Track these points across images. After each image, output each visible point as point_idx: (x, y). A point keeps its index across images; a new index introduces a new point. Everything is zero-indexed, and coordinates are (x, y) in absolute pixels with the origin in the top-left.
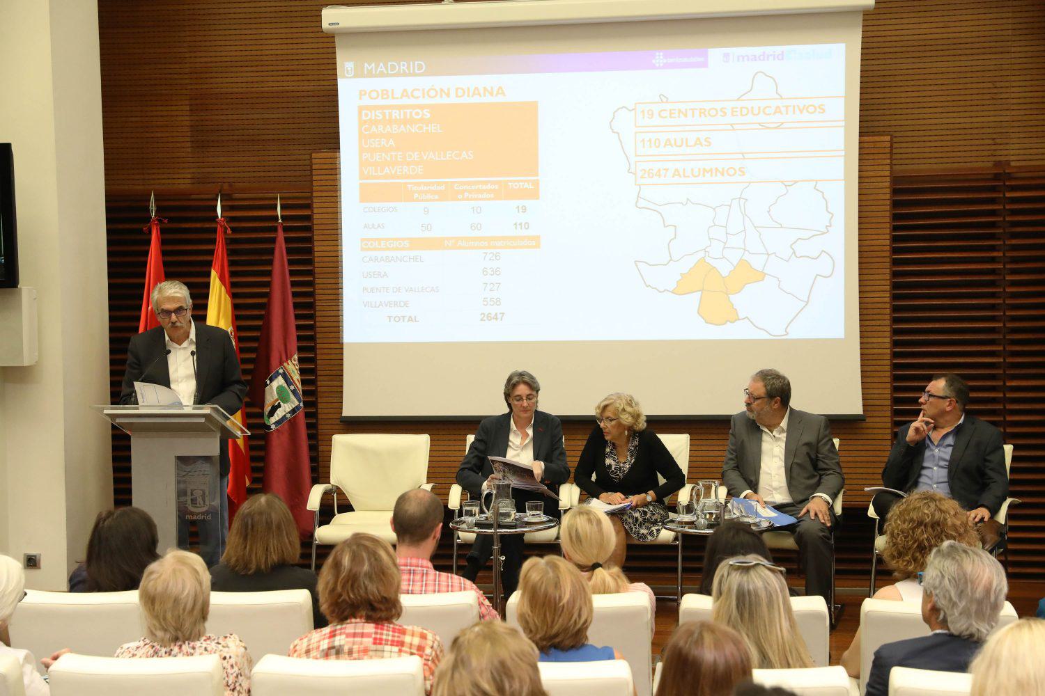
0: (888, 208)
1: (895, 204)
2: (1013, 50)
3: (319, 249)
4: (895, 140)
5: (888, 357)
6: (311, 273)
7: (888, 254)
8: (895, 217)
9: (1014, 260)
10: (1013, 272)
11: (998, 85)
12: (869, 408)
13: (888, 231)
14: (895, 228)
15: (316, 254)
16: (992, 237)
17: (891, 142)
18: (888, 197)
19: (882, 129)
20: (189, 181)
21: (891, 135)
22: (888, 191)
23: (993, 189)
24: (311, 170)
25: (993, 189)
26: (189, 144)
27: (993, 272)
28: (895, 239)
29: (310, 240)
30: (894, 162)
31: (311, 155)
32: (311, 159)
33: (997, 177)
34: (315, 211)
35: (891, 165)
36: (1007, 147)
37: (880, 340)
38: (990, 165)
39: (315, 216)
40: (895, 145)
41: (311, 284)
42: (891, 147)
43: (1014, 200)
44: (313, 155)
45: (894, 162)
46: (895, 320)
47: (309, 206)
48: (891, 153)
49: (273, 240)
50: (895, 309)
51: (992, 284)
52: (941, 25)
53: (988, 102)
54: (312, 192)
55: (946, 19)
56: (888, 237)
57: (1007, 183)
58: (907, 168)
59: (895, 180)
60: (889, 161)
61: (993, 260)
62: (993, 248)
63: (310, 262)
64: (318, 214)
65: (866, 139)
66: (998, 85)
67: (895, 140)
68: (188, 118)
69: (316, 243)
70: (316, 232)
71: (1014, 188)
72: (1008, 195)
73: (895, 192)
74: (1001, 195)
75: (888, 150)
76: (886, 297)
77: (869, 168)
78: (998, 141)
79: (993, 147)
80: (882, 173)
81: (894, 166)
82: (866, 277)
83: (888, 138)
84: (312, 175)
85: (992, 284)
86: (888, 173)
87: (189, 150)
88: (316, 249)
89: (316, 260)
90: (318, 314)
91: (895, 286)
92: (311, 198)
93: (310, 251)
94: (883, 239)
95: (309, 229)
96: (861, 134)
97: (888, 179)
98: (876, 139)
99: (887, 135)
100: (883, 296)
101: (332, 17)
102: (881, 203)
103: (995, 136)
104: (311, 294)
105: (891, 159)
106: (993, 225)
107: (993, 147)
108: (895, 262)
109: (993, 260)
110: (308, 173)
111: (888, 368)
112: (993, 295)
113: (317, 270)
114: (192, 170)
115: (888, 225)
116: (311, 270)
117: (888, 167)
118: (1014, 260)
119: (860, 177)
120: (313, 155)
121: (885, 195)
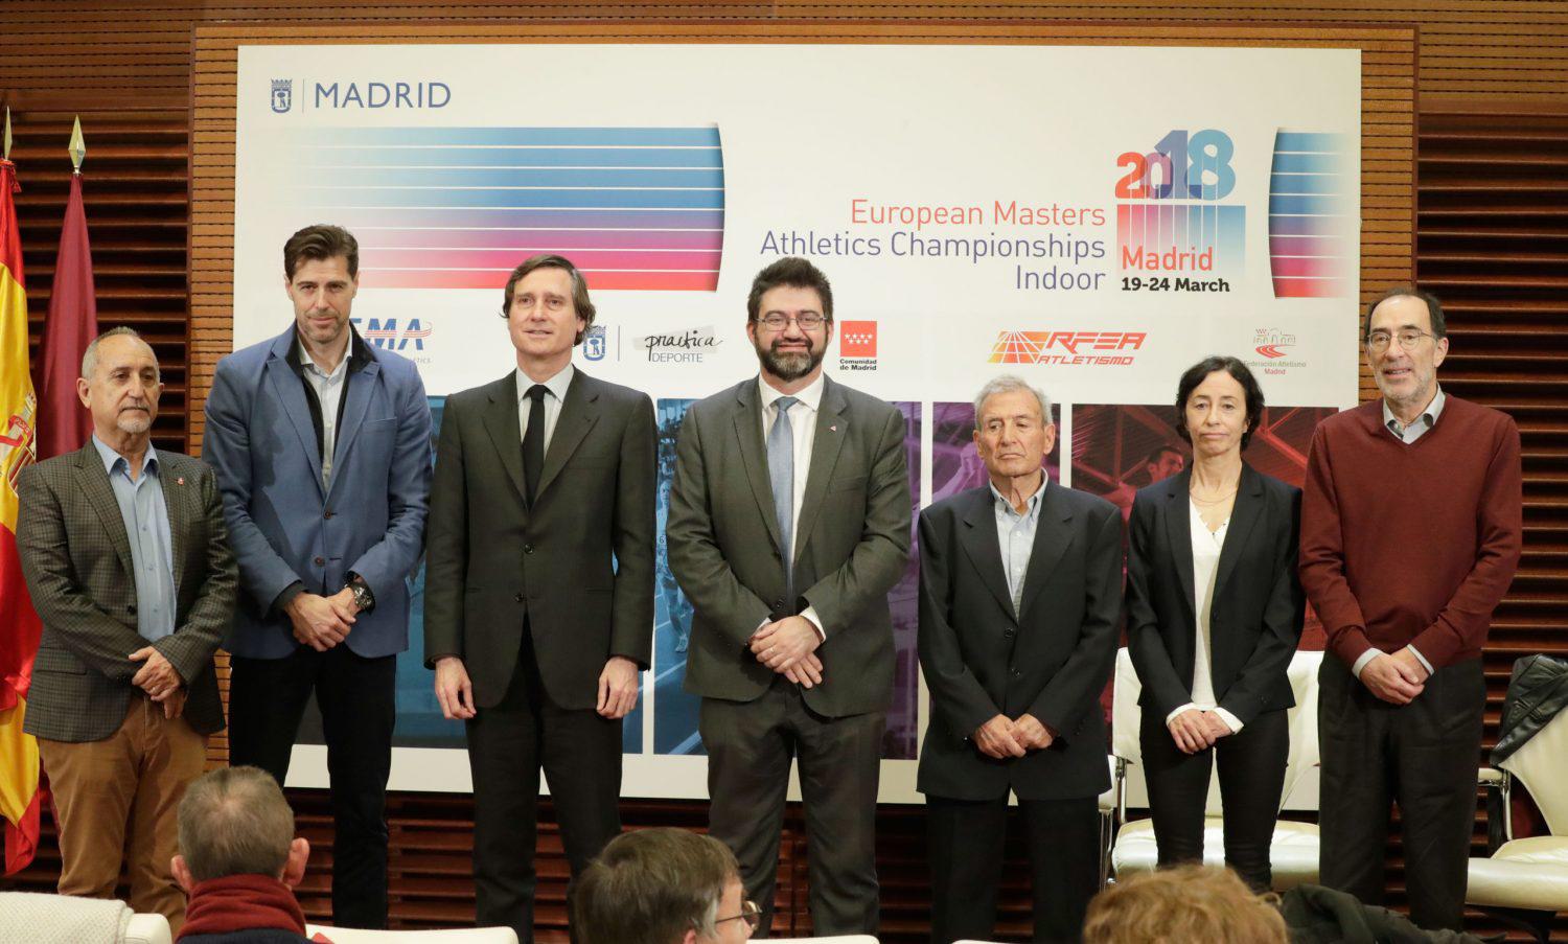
0: (1408, 178)
1: (1425, 172)
4: (1423, 39)
8: (1424, 199)
13: (1408, 226)
14: (1423, 222)
17: (1415, 40)
18: (1409, 154)
21: (1416, 29)
22: (1409, 142)
28: (1423, 244)
30: (1423, 85)
35: (1415, 88)
40: (1423, 51)
42: (1416, 52)
45: (1423, 85)
48: (1415, 64)
49: (60, 212)
56: (1408, 238)
58: (1444, 101)
60: (1410, 81)
67: (1423, 39)
73: (1424, 146)
75: (1409, 59)
80: (1398, 106)
81: (1421, 94)
83: (1410, 33)
86: (1408, 106)
97: (1409, 118)
105: (1415, 76)
115: (1408, 214)
117: (1409, 94)
121: (1404, 154)
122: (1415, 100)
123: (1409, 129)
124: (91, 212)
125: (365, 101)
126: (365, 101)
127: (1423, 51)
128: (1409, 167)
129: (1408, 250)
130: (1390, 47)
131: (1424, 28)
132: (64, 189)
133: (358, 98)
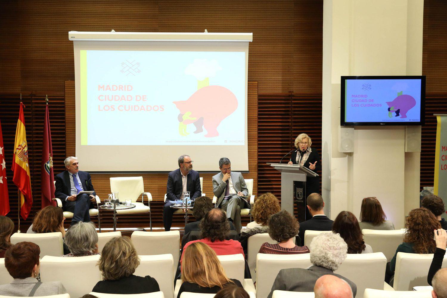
1: (259, 104)
2: (294, 56)
3: (68, 114)
4: (259, 83)
5: (257, 152)
6: (64, 122)
7: (257, 119)
8: (259, 108)
9: (294, 122)
10: (294, 126)
11: (290, 67)
12: (250, 169)
13: (257, 112)
14: (259, 111)
15: (66, 116)
16: (288, 115)
17: (258, 84)
18: (257, 101)
19: (255, 79)
20: (20, 89)
21: (258, 82)
22: (257, 99)
23: (288, 100)
24: (65, 87)
25: (288, 100)
26: (20, 77)
27: (288, 126)
28: (259, 115)
29: (64, 111)
31: (64, 82)
32: (65, 83)
33: (289, 96)
34: (66, 101)
35: (258, 91)
36: (292, 87)
37: (254, 147)
38: (288, 92)
39: (66, 103)
40: (259, 85)
41: (64, 126)
42: (258, 85)
43: (295, 103)
44: (65, 82)
45: (259, 90)
46: (259, 141)
47: (64, 99)
50: (259, 137)
51: (288, 129)
52: (273, 47)
53: (287, 72)
54: (65, 94)
55: (274, 46)
57: (293, 98)
59: (259, 96)
60: (257, 90)
61: (288, 122)
62: (288, 118)
63: (64, 118)
64: (67, 102)
65: (250, 82)
66: (290, 67)
67: (259, 83)
68: (20, 68)
69: (66, 112)
70: (66, 108)
71: (294, 100)
72: (293, 102)
73: (259, 100)
74: (291, 102)
75: (257, 86)
76: (256, 133)
77: (251, 92)
78: (290, 85)
79: (289, 87)
82: (250, 127)
83: (257, 82)
84: (65, 89)
85: (288, 129)
86: (257, 94)
87: (20, 79)
88: (66, 114)
89: (66, 118)
90: (67, 136)
91: (259, 130)
92: (64, 96)
93: (64, 115)
94: (255, 114)
95: (64, 107)
96: (248, 81)
97: (257, 95)
98: (253, 82)
99: (257, 81)
100: (255, 133)
101: (73, 35)
102: (255, 103)
103: (289, 83)
104: (64, 130)
106: (288, 111)
107: (289, 87)
108: (259, 122)
109: (288, 122)
110: (64, 88)
111: (257, 156)
112: (288, 133)
113: (66, 121)
114: (22, 86)
115: (257, 110)
116: (64, 121)
118: (294, 122)
119: (248, 95)
120: (65, 82)
121: (256, 101)
122: (258, 93)
123: (257, 97)
124: (50, 111)
125: (111, 89)
126: (111, 89)
127: (259, 85)
128: (257, 103)
129: (257, 116)
130: (254, 84)
131: (259, 81)
132: (45, 107)
133: (110, 89)
